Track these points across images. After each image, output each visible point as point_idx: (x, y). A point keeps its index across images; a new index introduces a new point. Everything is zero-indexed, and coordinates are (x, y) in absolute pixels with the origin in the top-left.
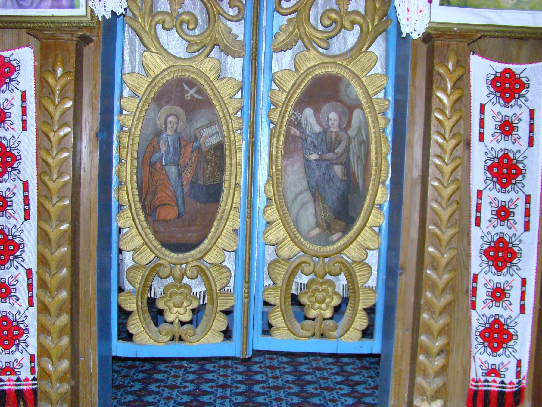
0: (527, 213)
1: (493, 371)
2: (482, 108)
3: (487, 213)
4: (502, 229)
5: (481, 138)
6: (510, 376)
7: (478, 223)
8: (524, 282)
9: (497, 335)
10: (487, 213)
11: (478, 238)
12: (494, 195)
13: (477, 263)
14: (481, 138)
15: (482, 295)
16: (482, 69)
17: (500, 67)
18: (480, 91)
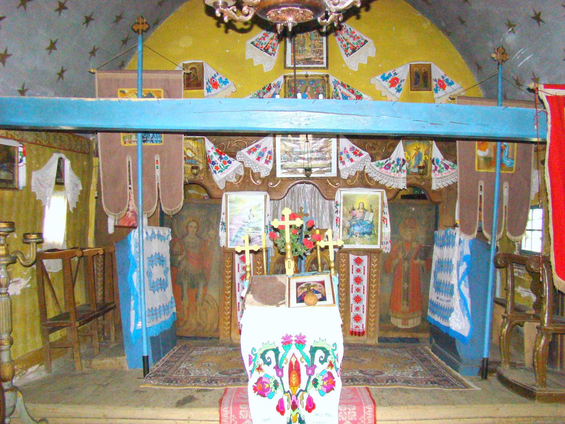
0: (364, 290)
1: (357, 327)
2: (353, 266)
3: (354, 290)
4: (358, 293)
5: (352, 273)
6: (361, 328)
7: (352, 292)
8: (363, 306)
9: (357, 318)
10: (354, 290)
11: (352, 296)
12: (356, 286)
13: (352, 301)
14: (352, 273)
15: (354, 309)
16: (352, 257)
17: (357, 257)
18: (352, 262)
